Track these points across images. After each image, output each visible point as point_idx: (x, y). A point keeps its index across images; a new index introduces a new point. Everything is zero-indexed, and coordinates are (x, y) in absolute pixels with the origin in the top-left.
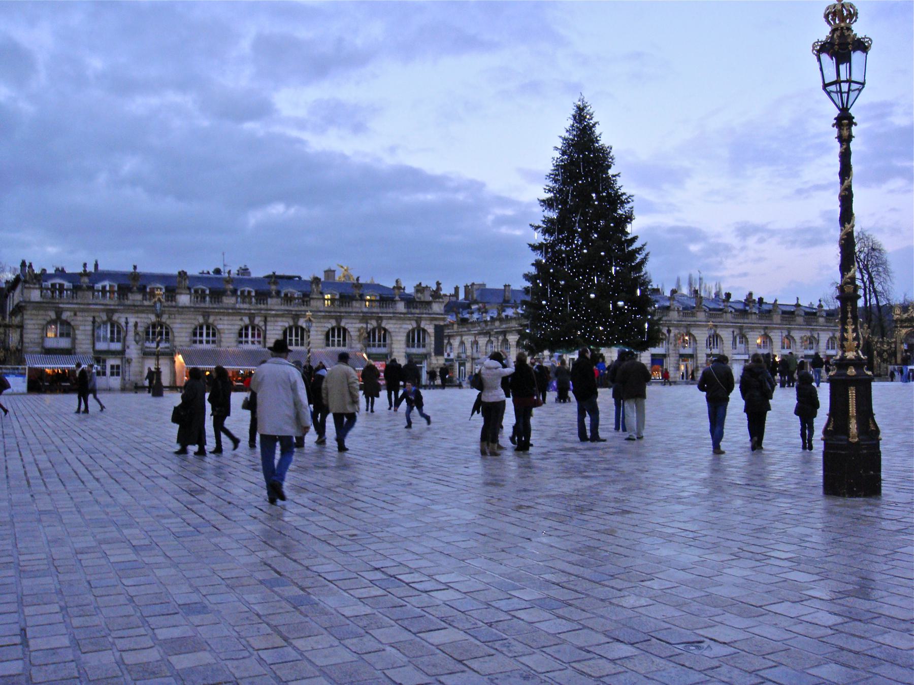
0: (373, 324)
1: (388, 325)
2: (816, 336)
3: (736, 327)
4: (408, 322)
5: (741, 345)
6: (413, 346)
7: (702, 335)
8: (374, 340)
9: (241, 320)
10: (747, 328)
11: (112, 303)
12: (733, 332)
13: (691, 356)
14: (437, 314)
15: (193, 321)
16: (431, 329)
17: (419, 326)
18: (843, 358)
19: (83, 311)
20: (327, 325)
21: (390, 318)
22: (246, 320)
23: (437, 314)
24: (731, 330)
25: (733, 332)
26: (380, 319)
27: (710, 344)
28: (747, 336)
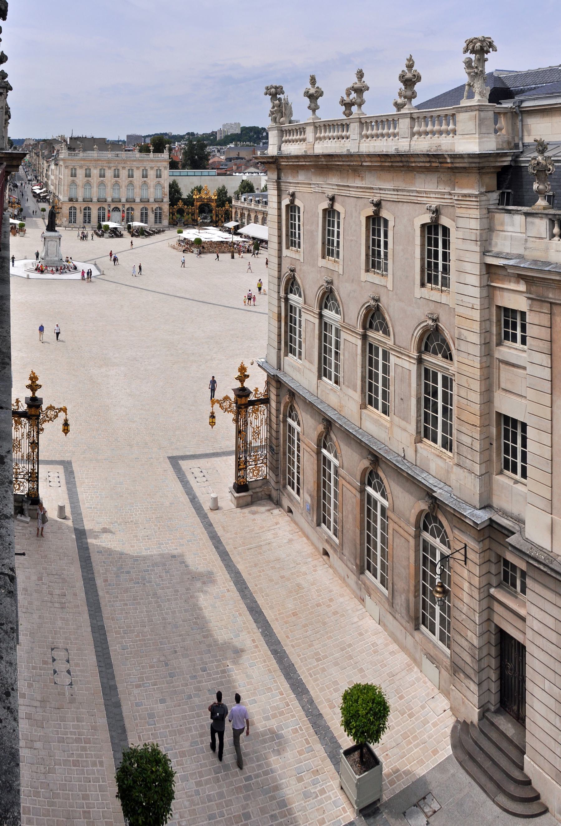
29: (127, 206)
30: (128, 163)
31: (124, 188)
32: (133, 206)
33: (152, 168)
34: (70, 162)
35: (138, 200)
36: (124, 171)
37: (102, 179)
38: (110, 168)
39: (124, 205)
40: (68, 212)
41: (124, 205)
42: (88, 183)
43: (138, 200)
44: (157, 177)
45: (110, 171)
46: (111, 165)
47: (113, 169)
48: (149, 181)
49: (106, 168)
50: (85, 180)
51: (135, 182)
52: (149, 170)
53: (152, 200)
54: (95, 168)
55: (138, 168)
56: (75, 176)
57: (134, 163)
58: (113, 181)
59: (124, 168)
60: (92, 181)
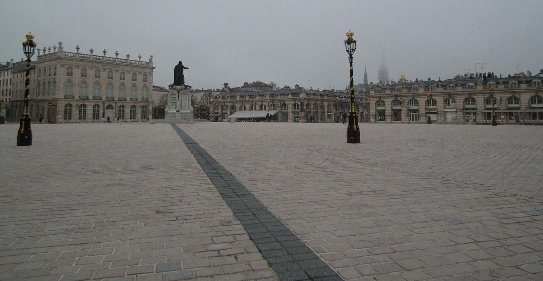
0: (283, 102)
1: (286, 103)
2: (518, 96)
3: (446, 94)
4: (292, 101)
5: (452, 104)
6: (296, 109)
7: (422, 101)
8: (284, 108)
9: (250, 103)
10: (454, 94)
11: (536, 88)
12: (444, 97)
13: (417, 110)
14: (503, 90)
15: (530, 95)
16: (299, 104)
17: (296, 102)
18: (352, 112)
19: (220, 103)
20: (507, 96)
21: (287, 100)
22: (251, 103)
23: (503, 90)
24: (443, 96)
25: (444, 97)
26: (284, 101)
27: (428, 103)
28: (455, 99)
29: (119, 104)
30: (121, 67)
31: (116, 88)
32: (124, 104)
33: (140, 73)
34: (67, 61)
35: (128, 99)
36: (117, 74)
37: (97, 79)
38: (104, 70)
39: (104, 103)
40: (63, 108)
41: (104, 103)
42: (84, 82)
43: (128, 99)
44: (143, 81)
45: (104, 73)
46: (106, 68)
47: (107, 71)
48: (137, 84)
49: (102, 70)
50: (82, 79)
51: (126, 83)
52: (138, 74)
53: (140, 100)
54: (91, 68)
55: (129, 72)
56: (71, 75)
57: (126, 68)
58: (107, 82)
59: (117, 71)
60: (88, 80)
